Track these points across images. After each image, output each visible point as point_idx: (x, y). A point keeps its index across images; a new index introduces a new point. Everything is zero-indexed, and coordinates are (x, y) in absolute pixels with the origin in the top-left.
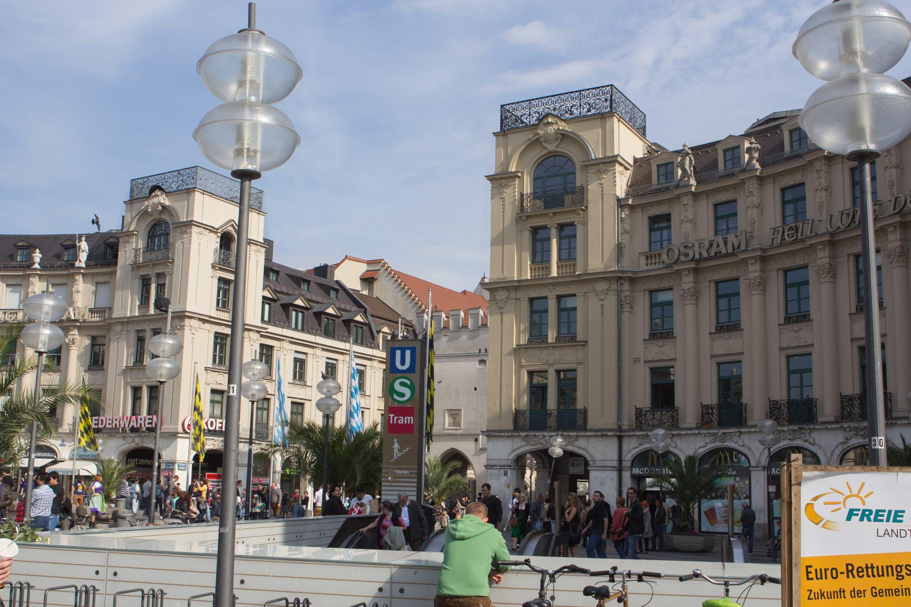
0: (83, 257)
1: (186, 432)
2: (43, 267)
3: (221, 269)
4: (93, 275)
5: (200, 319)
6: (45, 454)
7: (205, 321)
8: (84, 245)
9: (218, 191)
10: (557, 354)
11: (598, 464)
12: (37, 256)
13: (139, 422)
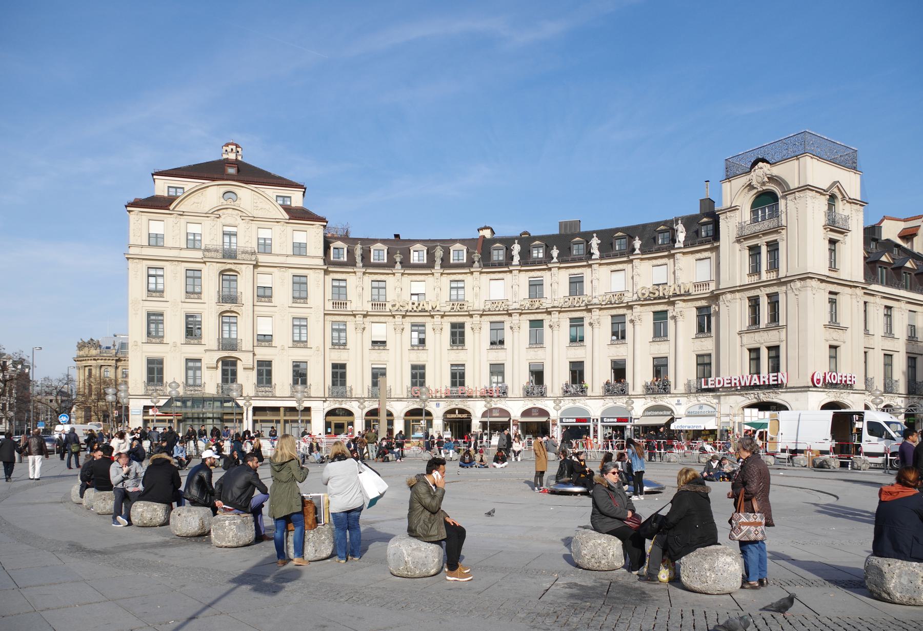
0: (681, 236)
1: (815, 386)
2: (643, 251)
3: (832, 230)
4: (692, 253)
5: (819, 279)
6: (661, 413)
7: (822, 281)
8: (680, 227)
9: (825, 157)
12: (637, 244)
13: (762, 380)
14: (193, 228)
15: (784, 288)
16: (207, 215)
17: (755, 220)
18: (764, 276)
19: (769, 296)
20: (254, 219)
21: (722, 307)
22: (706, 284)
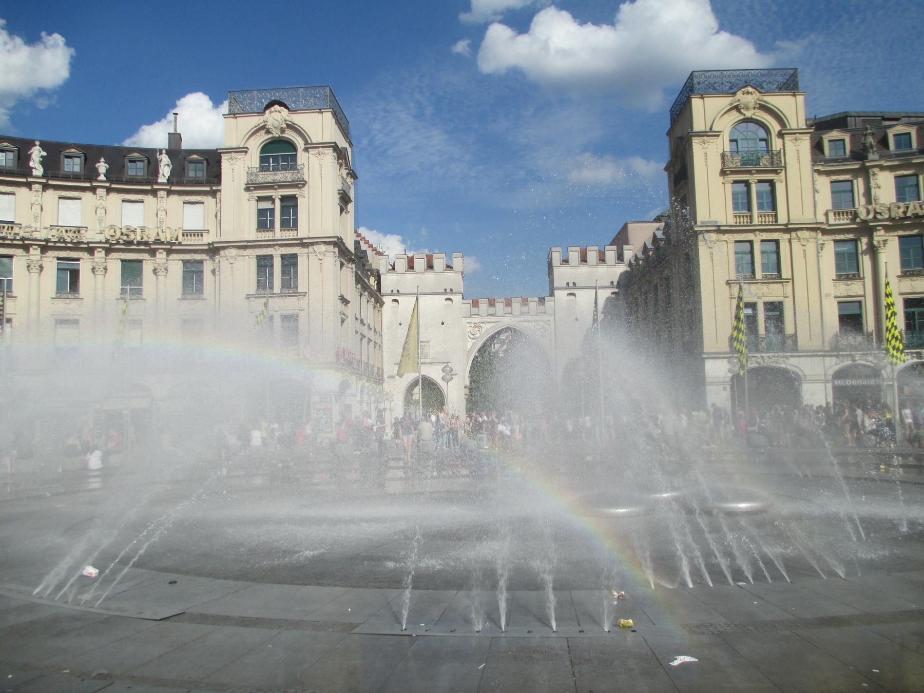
4: (180, 193)
10: (764, 289)
11: (808, 378)
12: (102, 167)
15: (305, 250)
17: (262, 169)
21: (225, 264)
22: (199, 233)
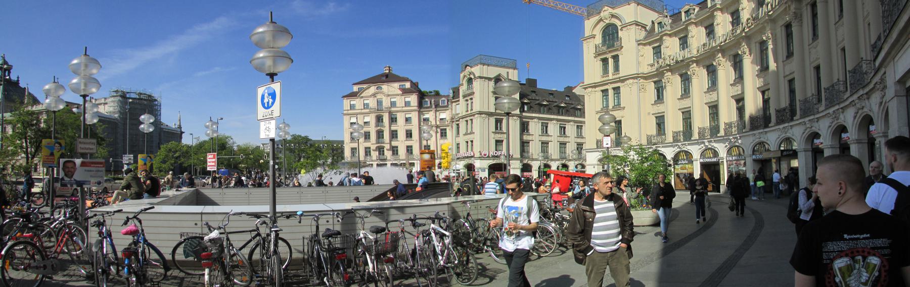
14: (366, 102)
16: (370, 96)
18: (611, 77)
19: (614, 89)
20: (389, 95)
